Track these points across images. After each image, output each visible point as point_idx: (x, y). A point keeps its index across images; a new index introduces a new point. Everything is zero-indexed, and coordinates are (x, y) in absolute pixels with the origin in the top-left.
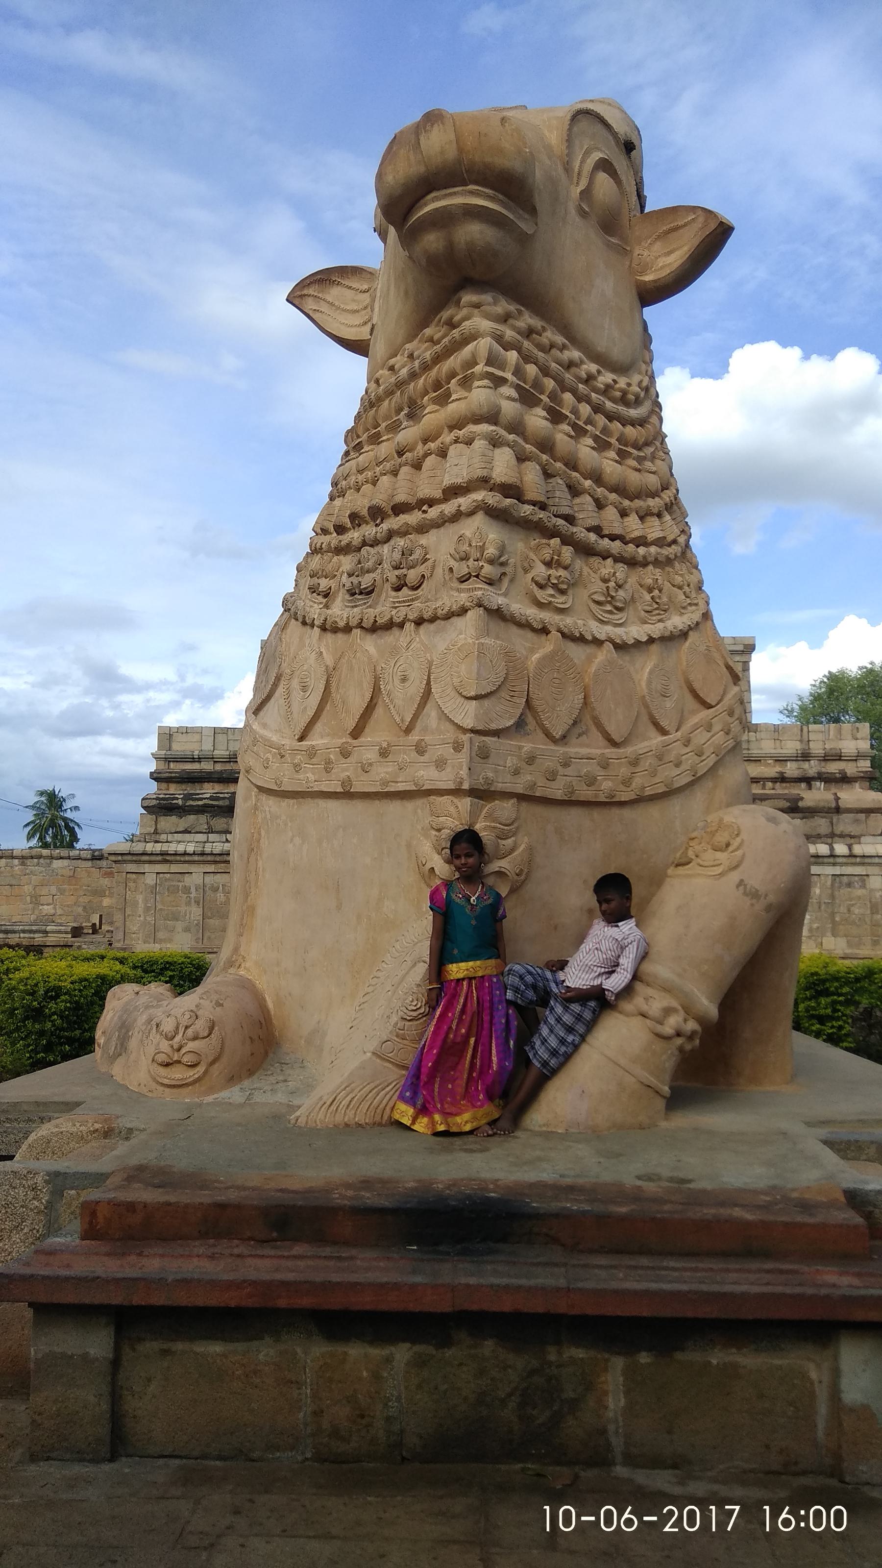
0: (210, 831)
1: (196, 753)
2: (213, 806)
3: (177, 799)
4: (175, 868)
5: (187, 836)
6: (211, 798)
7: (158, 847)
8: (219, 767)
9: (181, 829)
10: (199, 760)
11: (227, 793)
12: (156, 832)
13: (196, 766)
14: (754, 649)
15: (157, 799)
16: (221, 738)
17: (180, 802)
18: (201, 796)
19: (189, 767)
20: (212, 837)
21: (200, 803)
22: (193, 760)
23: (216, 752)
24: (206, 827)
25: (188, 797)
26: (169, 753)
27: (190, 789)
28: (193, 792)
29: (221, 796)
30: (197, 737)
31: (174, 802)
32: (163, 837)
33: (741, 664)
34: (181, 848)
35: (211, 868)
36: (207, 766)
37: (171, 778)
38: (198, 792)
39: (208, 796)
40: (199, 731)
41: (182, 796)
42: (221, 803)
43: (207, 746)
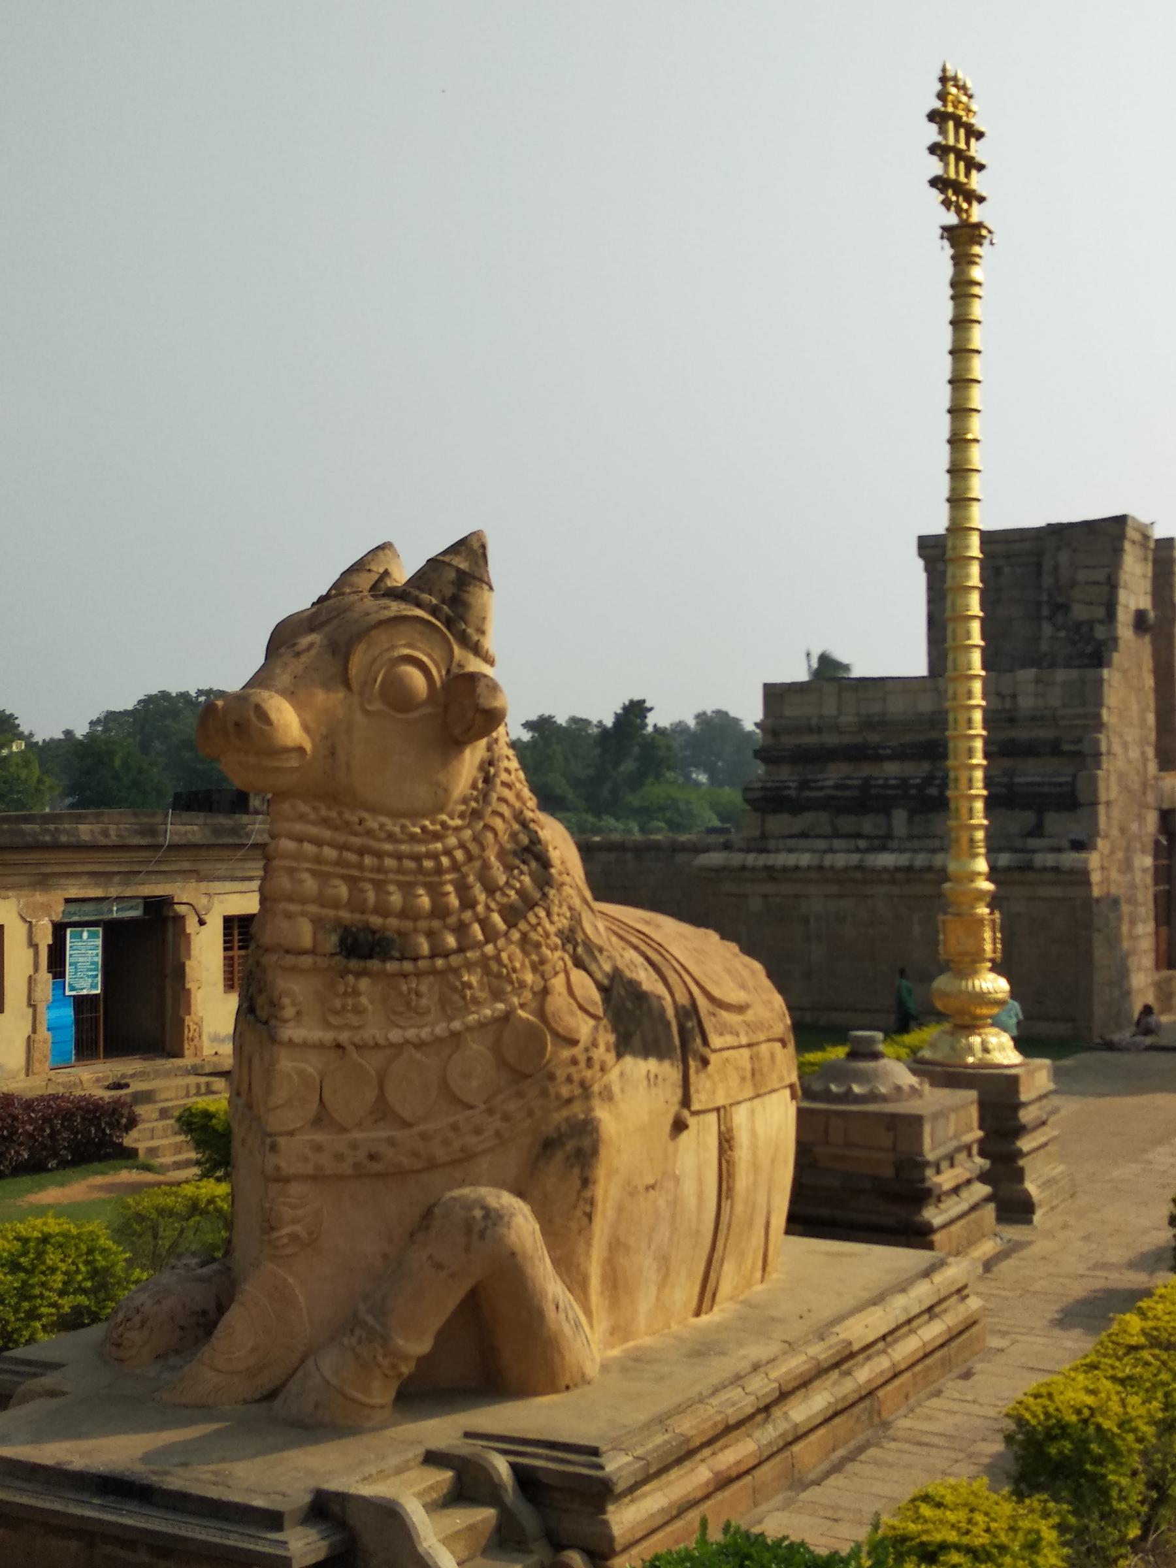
0: (837, 835)
3: (789, 788)
4: (786, 889)
5: (803, 843)
6: (836, 787)
7: (762, 860)
8: (846, 740)
10: (820, 730)
11: (857, 778)
12: (764, 837)
15: (763, 788)
17: (793, 793)
18: (820, 784)
20: (837, 843)
22: (810, 730)
25: (804, 785)
28: (810, 777)
29: (849, 782)
31: (785, 793)
32: (772, 844)
34: (790, 859)
35: (834, 889)
36: (830, 739)
38: (819, 776)
39: (830, 783)
42: (848, 793)
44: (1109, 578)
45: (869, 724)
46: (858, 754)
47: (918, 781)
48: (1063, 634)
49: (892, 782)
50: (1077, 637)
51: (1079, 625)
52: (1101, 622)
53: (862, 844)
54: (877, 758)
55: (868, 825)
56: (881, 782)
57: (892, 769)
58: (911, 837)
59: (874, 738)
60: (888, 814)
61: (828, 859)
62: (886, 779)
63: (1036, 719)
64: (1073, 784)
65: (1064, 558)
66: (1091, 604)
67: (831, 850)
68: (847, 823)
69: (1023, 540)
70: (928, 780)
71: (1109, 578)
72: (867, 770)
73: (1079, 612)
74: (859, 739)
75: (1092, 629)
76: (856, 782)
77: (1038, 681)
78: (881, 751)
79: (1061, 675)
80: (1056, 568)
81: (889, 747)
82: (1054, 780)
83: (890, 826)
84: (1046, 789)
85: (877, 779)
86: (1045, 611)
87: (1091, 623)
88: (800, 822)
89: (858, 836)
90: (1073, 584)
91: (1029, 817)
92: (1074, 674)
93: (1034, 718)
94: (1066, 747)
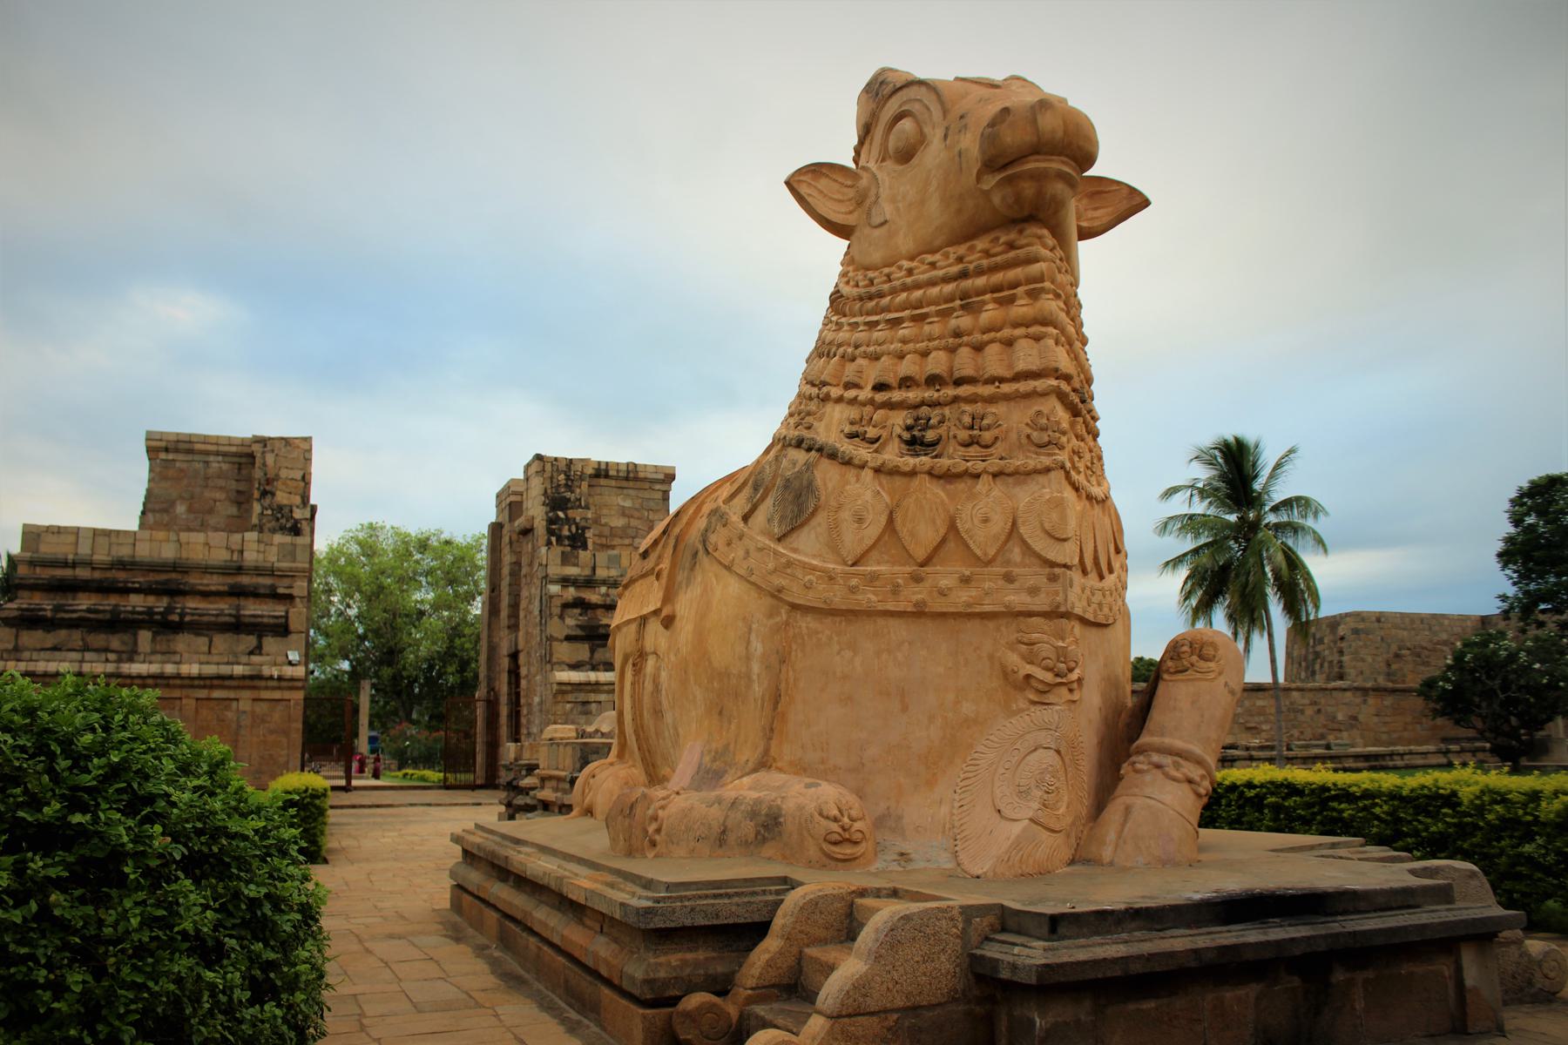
0: (86, 648)
1: (71, 557)
2: (89, 620)
3: (45, 610)
6: (89, 611)
8: (97, 575)
9: (49, 645)
12: (16, 649)
13: (68, 573)
14: (674, 479)
16: (101, 540)
17: (49, 614)
19: (59, 573)
20: (88, 656)
21: (75, 615)
22: (65, 564)
23: (96, 557)
24: (81, 643)
25: (57, 609)
26: (35, 555)
27: (59, 600)
29: (101, 608)
30: (72, 539)
31: (41, 613)
32: (26, 655)
33: (661, 493)
36: (83, 573)
37: (37, 584)
38: (71, 602)
39: (84, 607)
40: (77, 532)
41: (50, 607)
42: (100, 616)
43: (84, 550)
44: (304, 478)
45: (121, 564)
46: (103, 588)
47: (162, 609)
48: (269, 512)
49: (138, 609)
50: (279, 515)
51: (280, 508)
52: (298, 507)
53: (112, 656)
54: (126, 591)
55: (115, 642)
56: (130, 609)
57: (137, 602)
58: (154, 652)
59: (122, 576)
60: (135, 636)
61: (86, 668)
62: (134, 607)
63: (258, 571)
64: (286, 617)
65: (270, 459)
66: (290, 493)
67: (82, 661)
68: (99, 639)
69: (230, 445)
70: (169, 610)
71: (304, 478)
72: (113, 600)
73: (281, 497)
74: (109, 574)
75: (291, 511)
76: (107, 608)
77: (259, 541)
78: (130, 585)
79: (279, 538)
80: (264, 464)
81: (138, 582)
82: (272, 614)
83: (136, 643)
84: (265, 620)
85: (125, 606)
86: (256, 494)
87: (291, 506)
88: (51, 639)
89: (107, 650)
90: (277, 478)
91: (250, 641)
92: (288, 539)
93: (256, 568)
94: (281, 591)
